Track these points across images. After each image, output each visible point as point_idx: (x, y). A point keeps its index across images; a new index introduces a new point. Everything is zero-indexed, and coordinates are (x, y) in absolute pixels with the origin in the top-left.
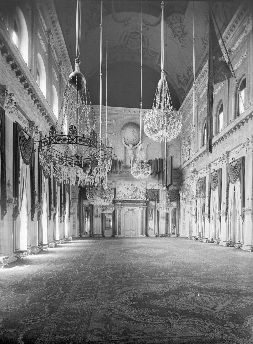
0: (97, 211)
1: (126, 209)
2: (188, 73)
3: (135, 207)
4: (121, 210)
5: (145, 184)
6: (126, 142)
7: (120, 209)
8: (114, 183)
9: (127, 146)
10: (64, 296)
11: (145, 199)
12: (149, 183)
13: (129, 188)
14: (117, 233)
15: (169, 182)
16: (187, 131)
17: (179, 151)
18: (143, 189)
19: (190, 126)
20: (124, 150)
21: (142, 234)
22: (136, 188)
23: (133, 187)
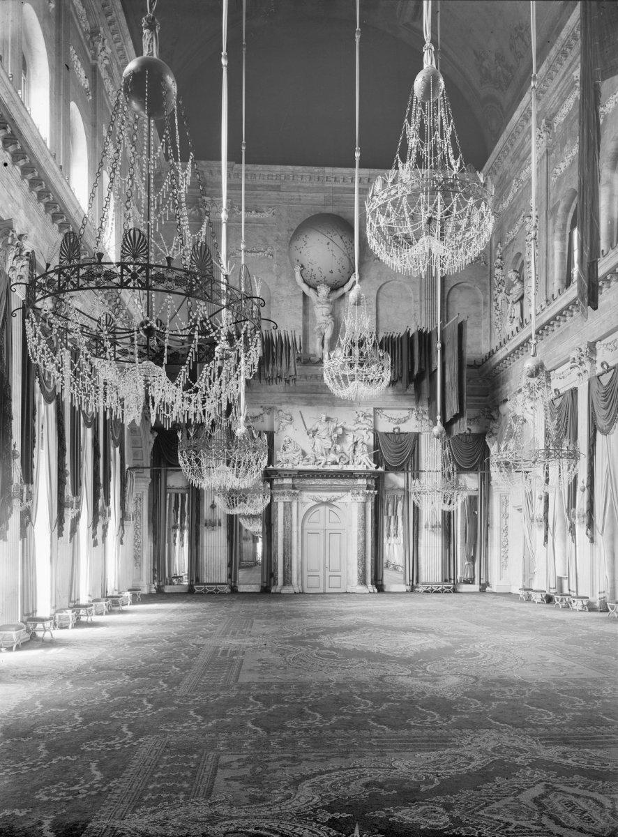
0: (213, 506)
1: (308, 498)
2: (512, 47)
3: (339, 494)
4: (290, 503)
5: (370, 416)
6: (307, 278)
7: (287, 499)
8: (268, 413)
9: (310, 293)
10: (105, 789)
11: (373, 467)
12: (385, 412)
13: (317, 430)
14: (280, 581)
15: (453, 408)
16: (510, 236)
17: (485, 304)
18: (364, 432)
19: (520, 221)
20: (302, 305)
21: (363, 582)
22: (340, 431)
23: (332, 426)
